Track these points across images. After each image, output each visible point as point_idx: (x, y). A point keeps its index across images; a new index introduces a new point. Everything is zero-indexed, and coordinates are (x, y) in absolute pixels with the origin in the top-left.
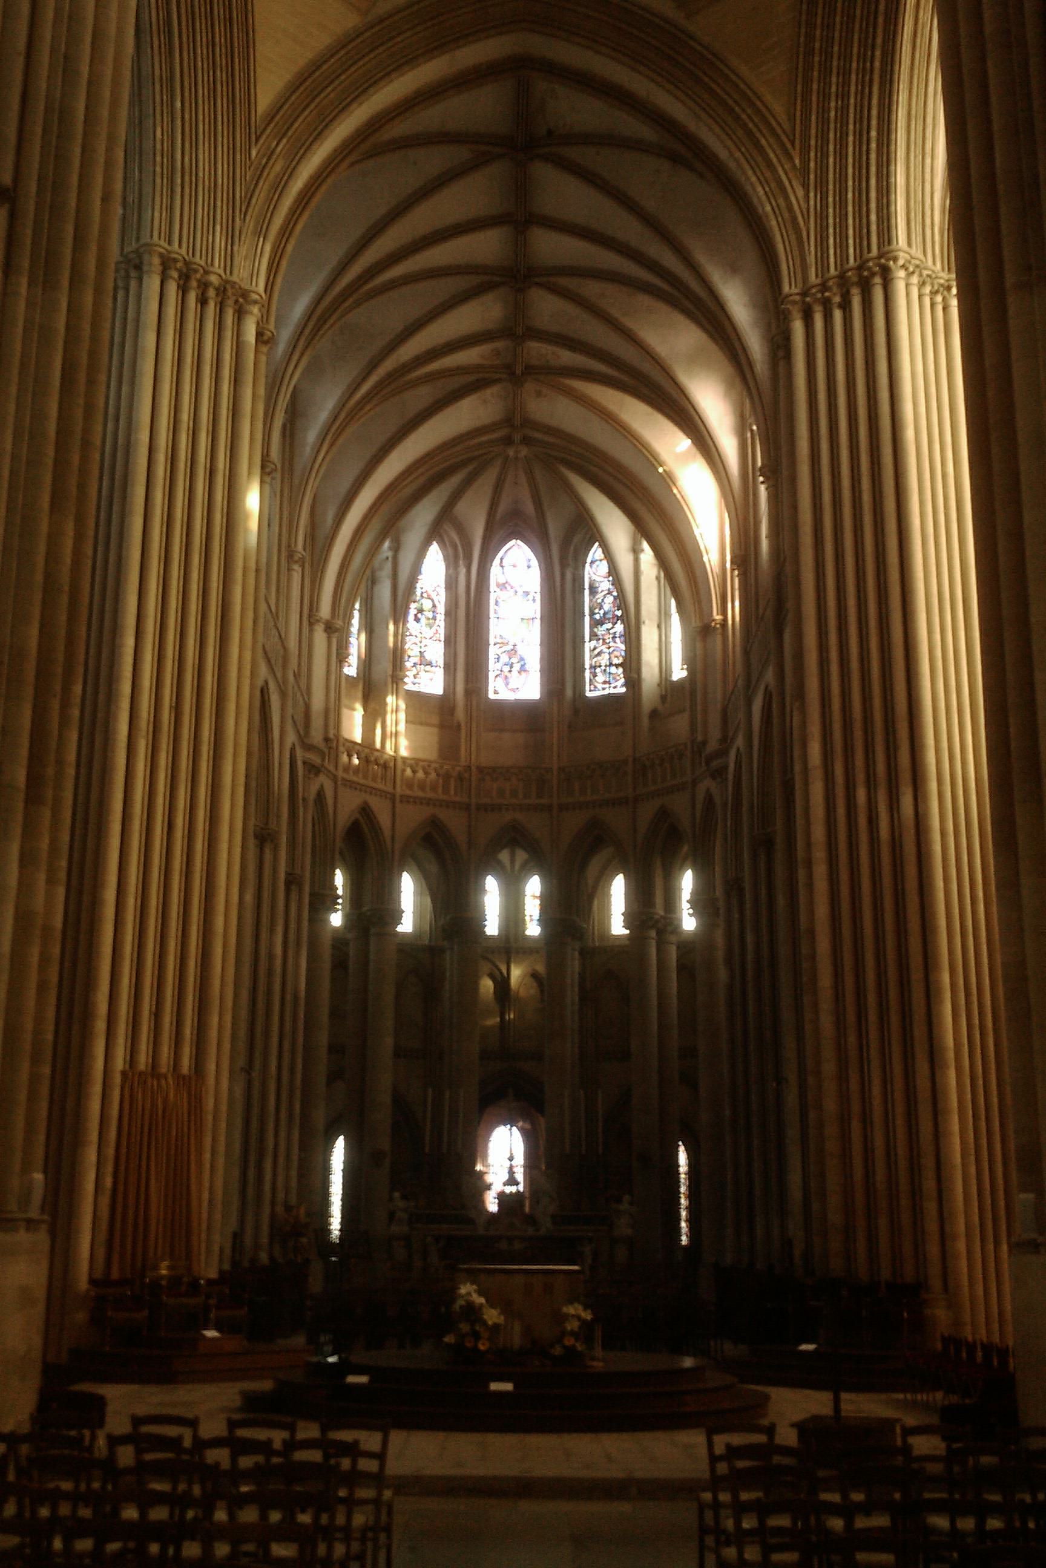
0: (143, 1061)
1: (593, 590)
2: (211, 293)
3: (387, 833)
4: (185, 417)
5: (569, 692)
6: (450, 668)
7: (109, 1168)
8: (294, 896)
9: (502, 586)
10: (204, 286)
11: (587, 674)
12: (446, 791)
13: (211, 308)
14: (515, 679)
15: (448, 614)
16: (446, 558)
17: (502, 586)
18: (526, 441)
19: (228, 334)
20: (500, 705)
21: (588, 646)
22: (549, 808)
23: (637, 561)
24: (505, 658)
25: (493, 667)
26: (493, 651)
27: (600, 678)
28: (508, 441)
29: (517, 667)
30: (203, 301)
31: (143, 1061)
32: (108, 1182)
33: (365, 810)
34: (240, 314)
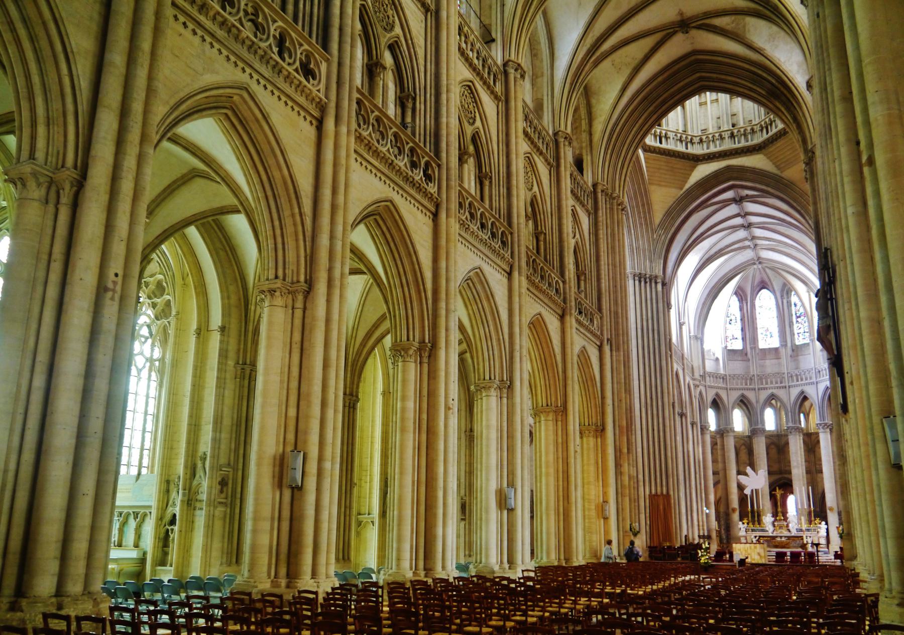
0: (653, 492)
1: (795, 305)
2: (648, 280)
3: (726, 402)
4: (644, 317)
5: (789, 344)
6: (744, 339)
7: (648, 519)
8: (695, 428)
9: (761, 307)
10: (645, 279)
11: (796, 336)
12: (746, 384)
13: (648, 285)
14: (769, 339)
15: (741, 320)
16: (739, 300)
17: (761, 307)
18: (760, 263)
19: (654, 290)
20: (764, 350)
21: (795, 326)
22: (786, 387)
23: (809, 295)
24: (764, 333)
25: (760, 337)
26: (760, 331)
27: (801, 337)
28: (754, 264)
29: (769, 335)
30: (646, 282)
31: (653, 492)
32: (648, 522)
33: (717, 395)
34: (656, 283)
